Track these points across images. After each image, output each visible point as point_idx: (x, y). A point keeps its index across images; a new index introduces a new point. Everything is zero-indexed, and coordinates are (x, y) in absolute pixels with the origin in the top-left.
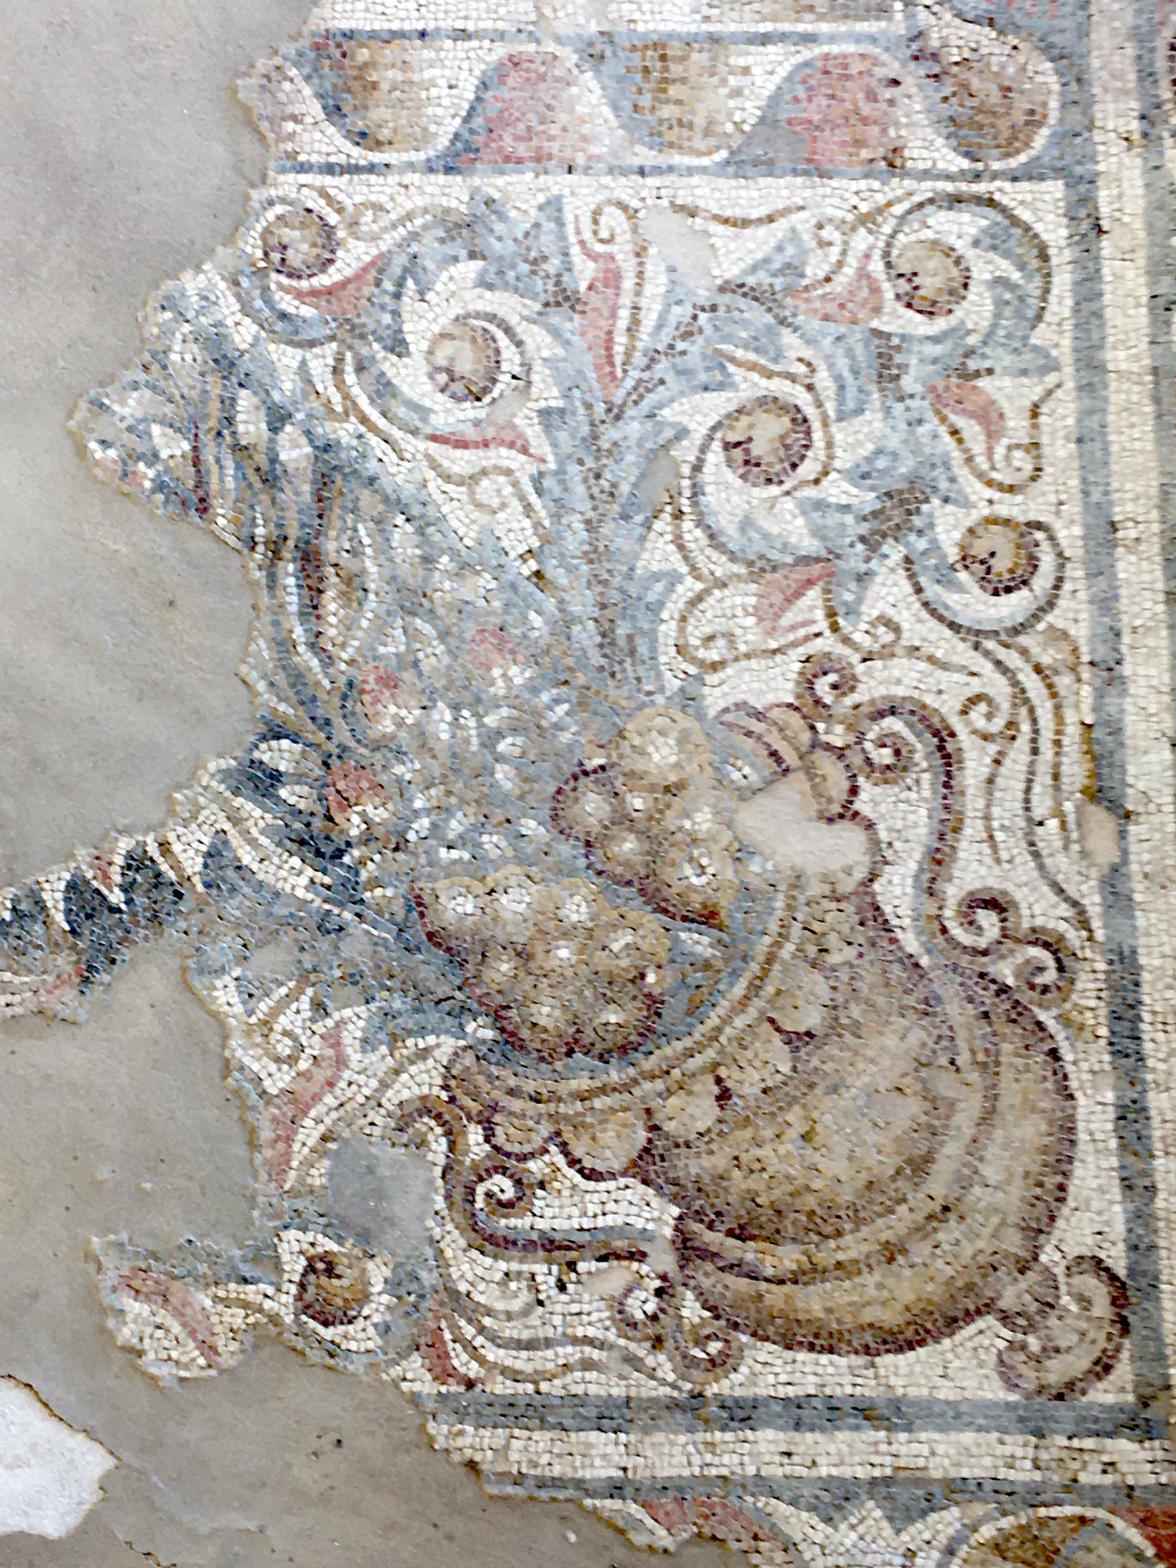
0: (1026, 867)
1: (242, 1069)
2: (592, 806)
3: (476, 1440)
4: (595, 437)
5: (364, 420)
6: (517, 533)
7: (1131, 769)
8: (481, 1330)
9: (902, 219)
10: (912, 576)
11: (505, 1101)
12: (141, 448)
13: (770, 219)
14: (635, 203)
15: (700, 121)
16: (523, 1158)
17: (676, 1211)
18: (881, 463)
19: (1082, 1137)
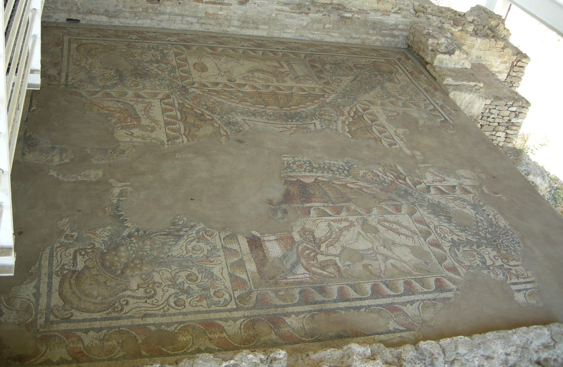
0: (132, 307)
2: (138, 262)
3: (48, 251)
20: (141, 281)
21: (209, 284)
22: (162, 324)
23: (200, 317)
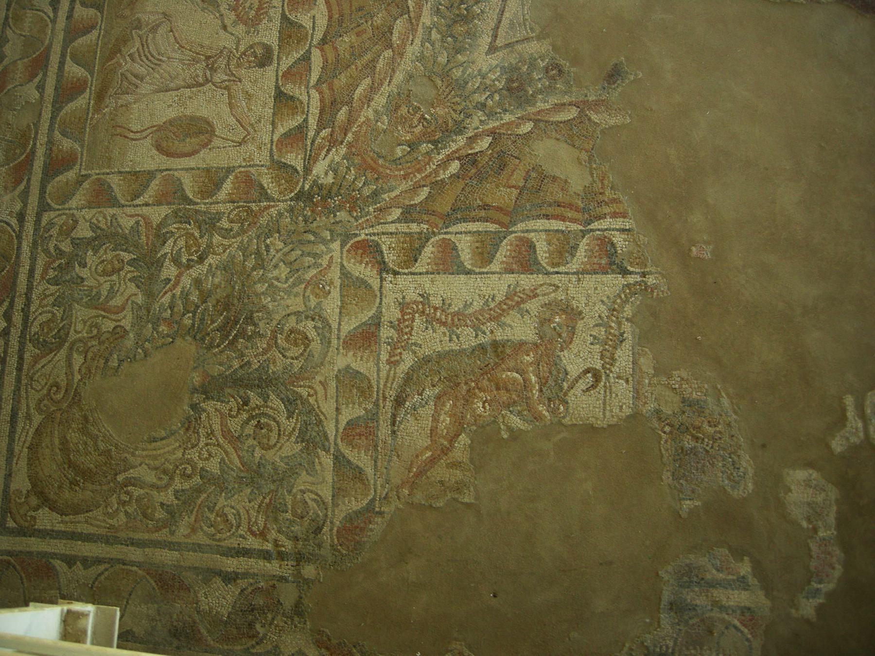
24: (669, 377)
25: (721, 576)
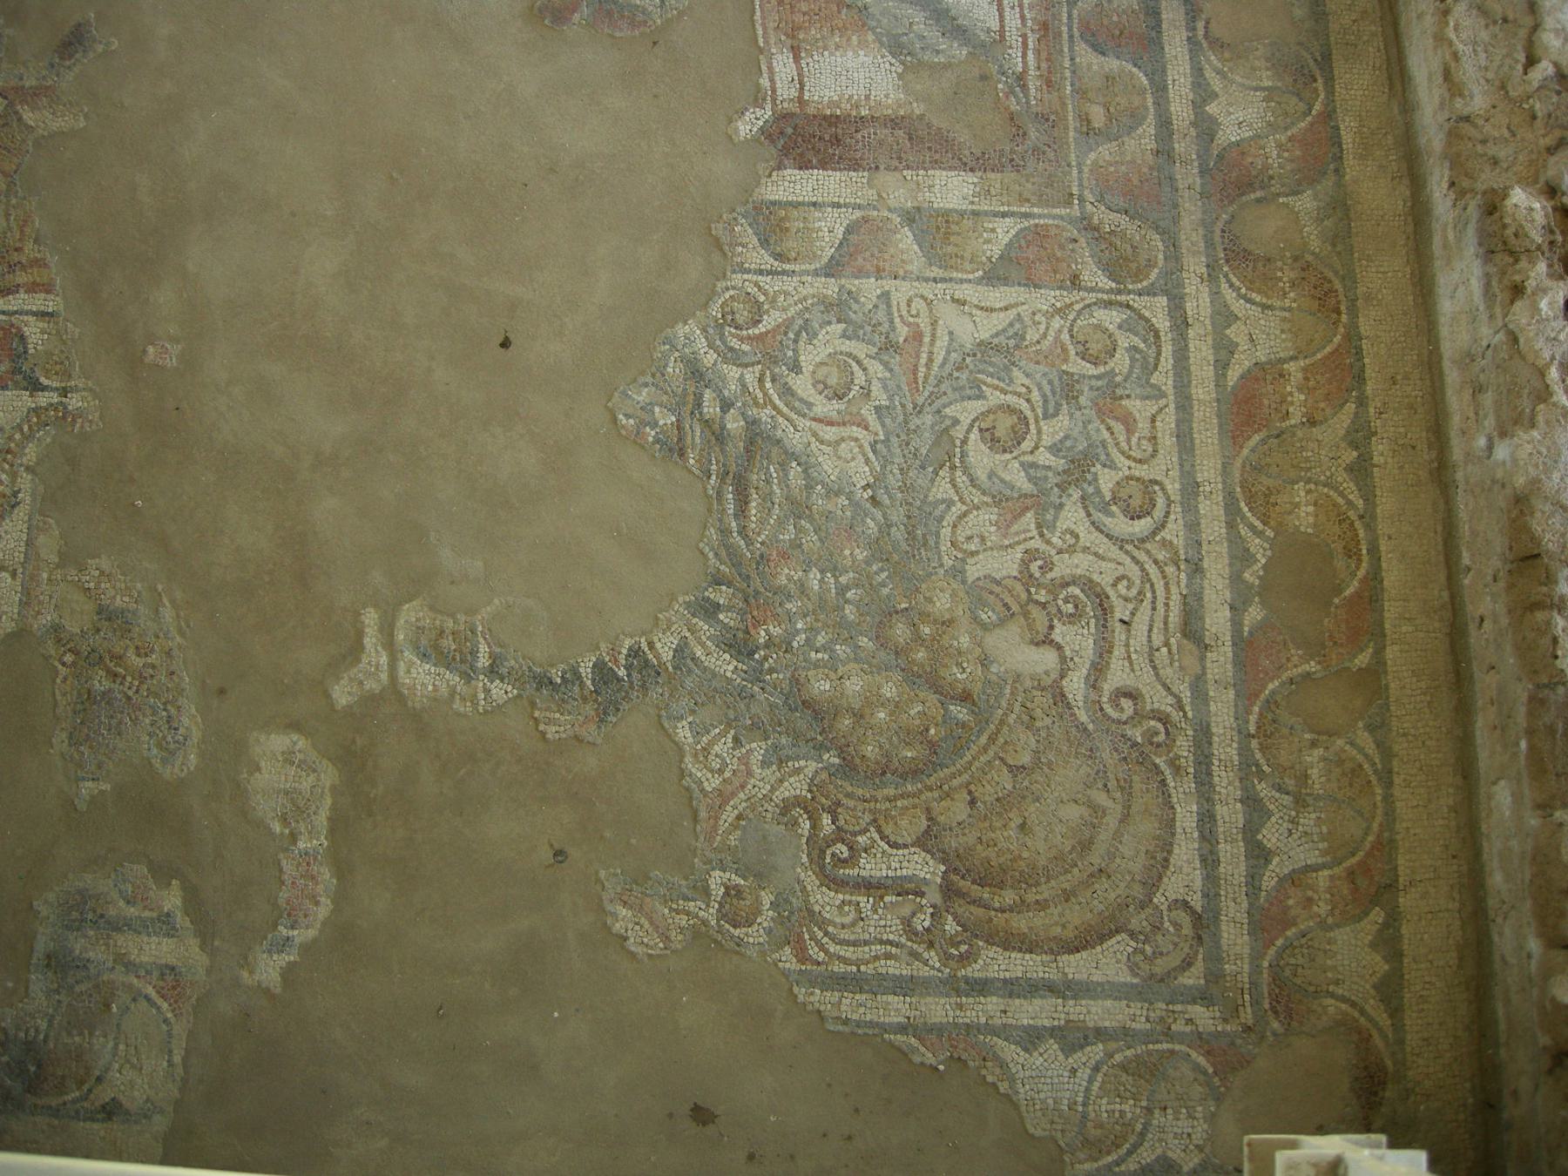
1: (690, 775)
2: (901, 632)
3: (819, 998)
4: (906, 422)
5: (775, 407)
6: (861, 473)
7: (1208, 621)
8: (826, 934)
9: (1079, 313)
10: (1085, 508)
11: (844, 801)
12: (648, 418)
13: (1006, 309)
14: (931, 296)
15: (967, 255)
16: (855, 834)
17: (943, 868)
18: (1068, 443)
19: (1179, 830)
20: (1014, 629)
21: (1042, 368)
22: (1236, 579)
23: (1207, 435)
24: (82, 569)
25: (132, 911)
